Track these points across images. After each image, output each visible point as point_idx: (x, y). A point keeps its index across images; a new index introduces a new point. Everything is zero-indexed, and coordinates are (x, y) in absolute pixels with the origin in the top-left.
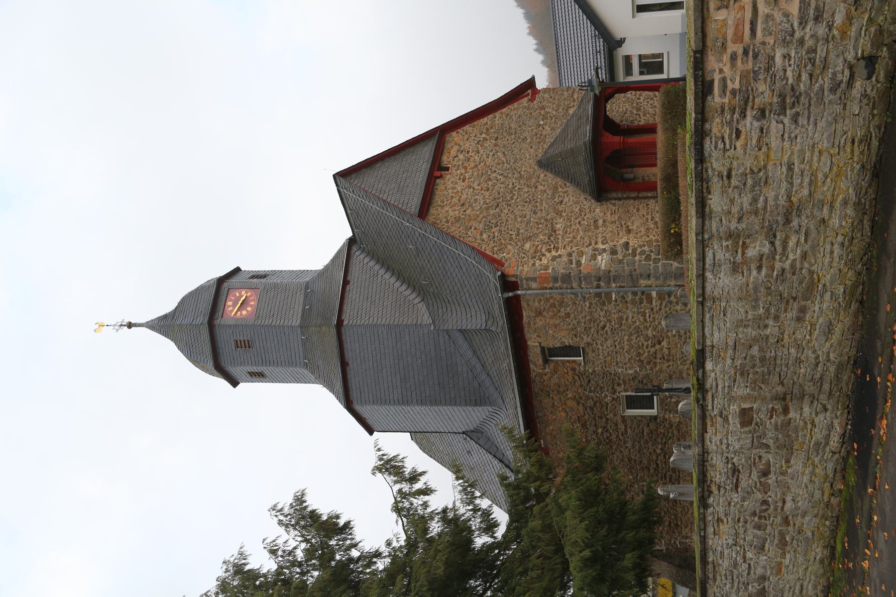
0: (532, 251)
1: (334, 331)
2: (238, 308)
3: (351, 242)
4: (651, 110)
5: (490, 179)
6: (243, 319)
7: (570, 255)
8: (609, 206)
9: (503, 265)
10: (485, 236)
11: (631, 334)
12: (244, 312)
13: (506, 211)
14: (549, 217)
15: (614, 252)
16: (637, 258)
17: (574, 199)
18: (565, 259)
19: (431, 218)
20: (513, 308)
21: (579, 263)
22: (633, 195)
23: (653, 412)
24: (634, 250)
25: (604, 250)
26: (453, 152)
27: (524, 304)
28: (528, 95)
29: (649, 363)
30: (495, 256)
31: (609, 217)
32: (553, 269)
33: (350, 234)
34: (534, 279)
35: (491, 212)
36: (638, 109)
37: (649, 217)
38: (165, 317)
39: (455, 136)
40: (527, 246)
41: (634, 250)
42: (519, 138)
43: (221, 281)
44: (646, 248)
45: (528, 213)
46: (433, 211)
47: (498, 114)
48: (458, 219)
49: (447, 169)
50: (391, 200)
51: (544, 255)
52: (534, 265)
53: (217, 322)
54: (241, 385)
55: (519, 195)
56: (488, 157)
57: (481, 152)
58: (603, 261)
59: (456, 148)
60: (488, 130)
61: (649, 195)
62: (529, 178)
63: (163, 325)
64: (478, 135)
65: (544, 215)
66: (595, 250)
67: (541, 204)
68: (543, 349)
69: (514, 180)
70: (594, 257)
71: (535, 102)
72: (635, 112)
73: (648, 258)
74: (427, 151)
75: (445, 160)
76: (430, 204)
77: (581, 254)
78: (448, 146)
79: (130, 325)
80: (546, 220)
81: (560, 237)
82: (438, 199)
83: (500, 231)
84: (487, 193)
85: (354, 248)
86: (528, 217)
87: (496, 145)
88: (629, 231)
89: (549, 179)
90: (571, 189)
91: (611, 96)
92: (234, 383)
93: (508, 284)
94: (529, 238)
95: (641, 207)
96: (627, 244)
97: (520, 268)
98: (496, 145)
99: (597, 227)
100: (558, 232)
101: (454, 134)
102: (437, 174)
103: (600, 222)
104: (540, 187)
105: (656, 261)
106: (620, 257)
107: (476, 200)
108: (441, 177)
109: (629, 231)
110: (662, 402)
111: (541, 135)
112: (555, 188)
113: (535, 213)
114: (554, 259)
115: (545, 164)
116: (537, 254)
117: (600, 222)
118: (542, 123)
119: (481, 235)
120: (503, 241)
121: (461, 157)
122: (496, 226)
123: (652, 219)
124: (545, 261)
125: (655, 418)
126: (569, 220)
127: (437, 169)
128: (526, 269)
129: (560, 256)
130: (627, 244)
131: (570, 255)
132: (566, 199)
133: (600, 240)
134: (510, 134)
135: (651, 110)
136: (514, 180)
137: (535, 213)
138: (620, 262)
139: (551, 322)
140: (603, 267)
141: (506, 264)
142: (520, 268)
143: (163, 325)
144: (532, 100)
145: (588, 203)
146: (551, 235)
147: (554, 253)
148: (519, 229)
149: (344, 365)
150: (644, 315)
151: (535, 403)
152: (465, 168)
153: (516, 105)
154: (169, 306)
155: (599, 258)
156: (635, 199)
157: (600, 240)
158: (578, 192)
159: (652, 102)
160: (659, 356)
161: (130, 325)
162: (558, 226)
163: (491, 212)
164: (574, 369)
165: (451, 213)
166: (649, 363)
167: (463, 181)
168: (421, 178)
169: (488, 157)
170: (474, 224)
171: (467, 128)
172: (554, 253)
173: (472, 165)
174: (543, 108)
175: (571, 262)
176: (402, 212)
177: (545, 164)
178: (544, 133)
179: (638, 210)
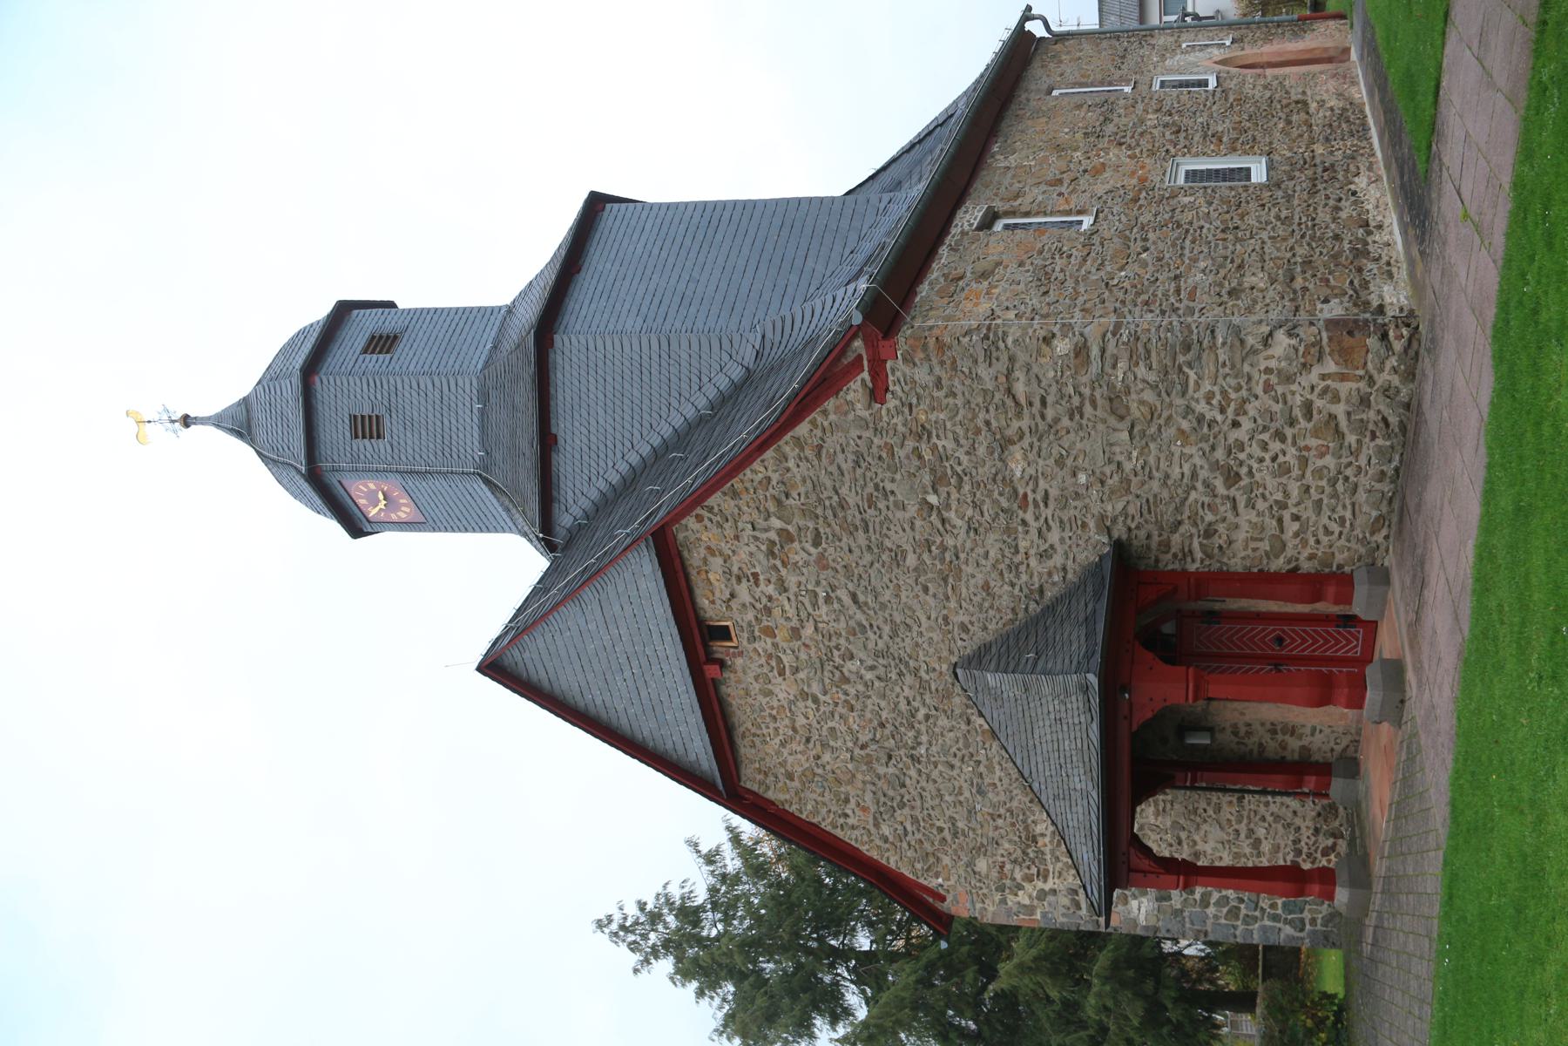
0: (994, 874)
4: (1271, 483)
5: (847, 680)
13: (913, 773)
14: (1015, 804)
16: (1211, 910)
28: (857, 365)
30: (921, 881)
32: (1044, 915)
36: (1232, 478)
37: (1243, 828)
42: (881, 546)
45: (965, 785)
46: (745, 750)
47: (786, 444)
49: (724, 633)
51: (1020, 887)
52: (1004, 901)
55: (933, 736)
56: (815, 605)
57: (792, 581)
60: (779, 503)
63: (240, 423)
64: (761, 523)
65: (1002, 797)
67: (990, 769)
69: (907, 692)
71: (892, 403)
72: (1219, 483)
75: (711, 607)
76: (730, 730)
79: (187, 421)
80: (1010, 810)
81: (1047, 850)
83: (915, 820)
84: (853, 718)
86: (967, 794)
94: (980, 850)
95: (1225, 806)
97: (979, 906)
100: (1041, 841)
101: (690, 521)
107: (832, 729)
111: (944, 548)
114: (1042, 895)
118: (933, 499)
119: (877, 825)
120: (929, 848)
122: (902, 805)
123: (1251, 832)
128: (991, 909)
129: (1054, 892)
135: (1271, 483)
136: (907, 692)
140: (1142, 920)
141: (949, 898)
142: (979, 906)
143: (240, 423)
144: (877, 393)
146: (1028, 846)
148: (953, 820)
159: (1276, 446)
161: (187, 421)
167: (782, 673)
169: (815, 605)
172: (1040, 884)
174: (923, 432)
178: (950, 542)
179: (1218, 809)
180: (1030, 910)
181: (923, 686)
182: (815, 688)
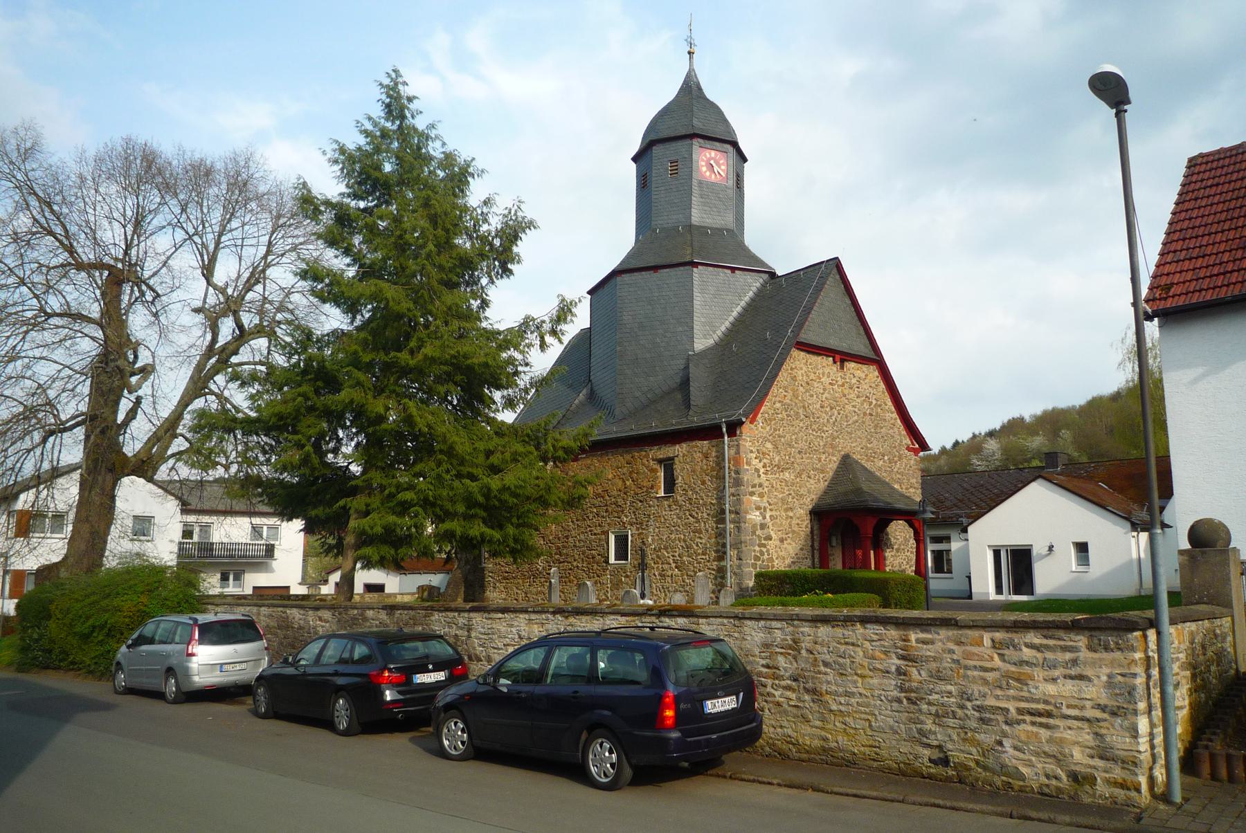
1: (688, 259)
2: (709, 164)
3: (772, 275)
6: (699, 170)
7: (761, 485)
8: (807, 522)
9: (751, 422)
10: (778, 405)
11: (685, 541)
12: (704, 169)
15: (763, 526)
16: (757, 548)
17: (813, 488)
18: (757, 481)
19: (795, 353)
20: (711, 432)
21: (752, 494)
22: (816, 545)
23: (612, 560)
24: (764, 546)
25: (764, 518)
26: (858, 373)
27: (714, 442)
29: (658, 557)
31: (795, 521)
33: (780, 273)
34: (738, 452)
35: (801, 411)
36: (898, 550)
38: (700, 89)
39: (872, 372)
40: (769, 445)
41: (764, 546)
43: (735, 144)
44: (766, 556)
46: (802, 354)
47: (895, 415)
48: (794, 378)
49: (842, 368)
50: (813, 314)
53: (696, 142)
54: (634, 166)
58: (754, 516)
59: (863, 376)
61: (816, 560)
62: (833, 447)
63: (691, 91)
66: (765, 509)
68: (672, 459)
70: (758, 508)
73: (757, 558)
74: (863, 349)
75: (851, 365)
76: (809, 352)
77: (761, 495)
78: (864, 367)
82: (814, 359)
85: (766, 276)
87: (865, 414)
88: (782, 540)
89: (833, 464)
90: (823, 485)
91: (911, 525)
92: (635, 159)
93: (734, 428)
96: (769, 538)
98: (865, 414)
99: (786, 510)
101: (877, 373)
102: (838, 357)
103: (791, 514)
104: (823, 457)
105: (754, 566)
106: (759, 532)
108: (835, 362)
109: (782, 540)
110: (623, 568)
112: (822, 471)
113: (800, 452)
114: (757, 470)
115: (846, 463)
116: (761, 455)
117: (791, 514)
121: (854, 381)
124: (755, 462)
125: (607, 562)
126: (793, 484)
127: (842, 357)
128: (748, 444)
129: (759, 476)
130: (769, 538)
131: (761, 485)
132: (812, 481)
133: (774, 513)
134: (876, 426)
137: (800, 452)
138: (754, 533)
139: (698, 468)
140: (749, 517)
143: (691, 91)
144: (908, 449)
145: (809, 502)
147: (762, 470)
149: (655, 268)
150: (704, 554)
151: (620, 450)
152: (843, 385)
153: (904, 432)
154: (711, 93)
155: (758, 513)
156: (812, 546)
157: (774, 513)
158: (820, 493)
160: (666, 566)
162: (787, 474)
163: (801, 411)
164: (652, 487)
165: (800, 373)
166: (658, 557)
168: (833, 343)
170: (790, 395)
171: (882, 386)
172: (762, 470)
173: (846, 392)
174: (900, 458)
175: (754, 486)
176: (800, 326)
177: (846, 463)
180: (749, 463)
181: (834, 439)
182: (826, 395)
